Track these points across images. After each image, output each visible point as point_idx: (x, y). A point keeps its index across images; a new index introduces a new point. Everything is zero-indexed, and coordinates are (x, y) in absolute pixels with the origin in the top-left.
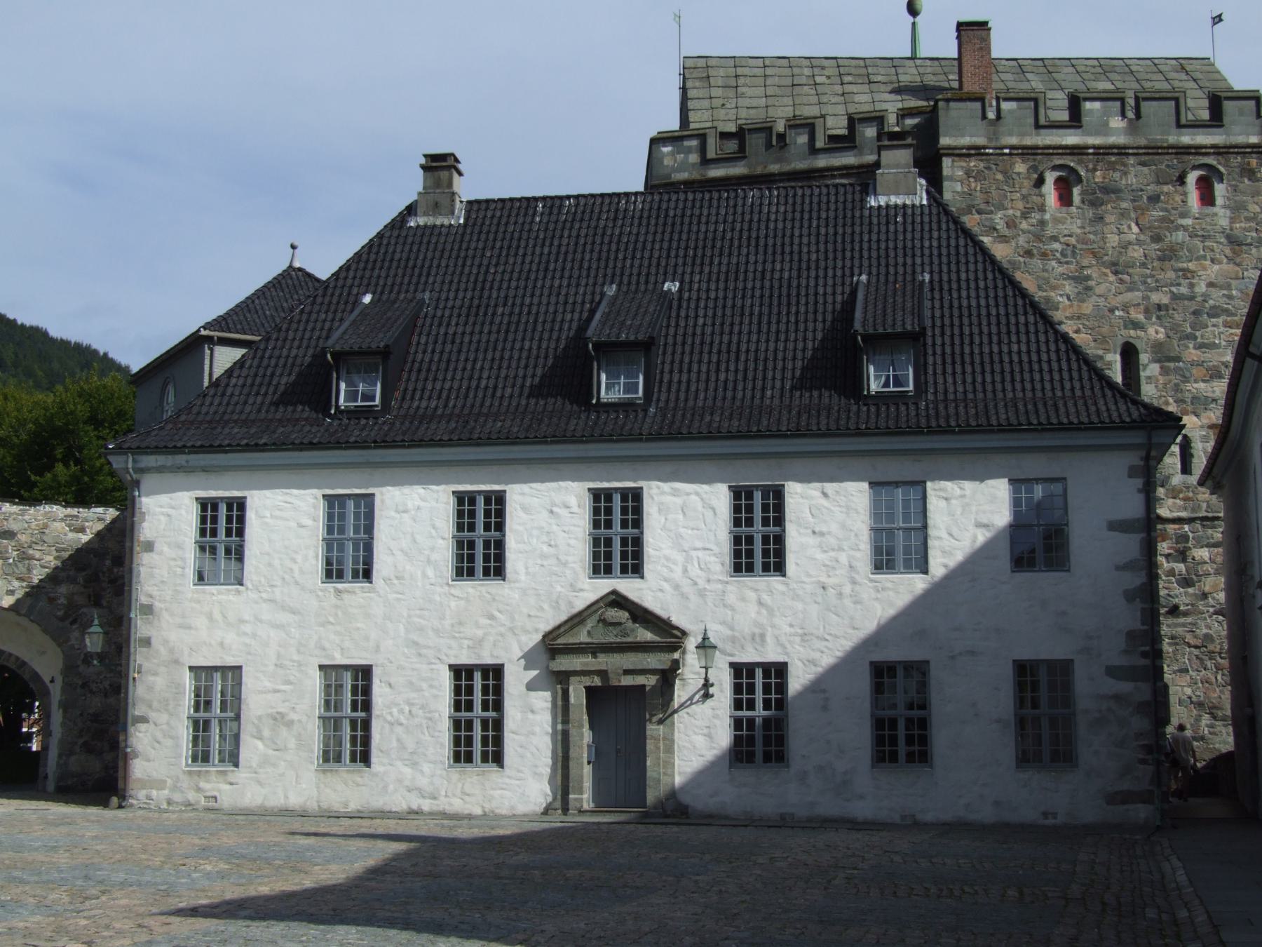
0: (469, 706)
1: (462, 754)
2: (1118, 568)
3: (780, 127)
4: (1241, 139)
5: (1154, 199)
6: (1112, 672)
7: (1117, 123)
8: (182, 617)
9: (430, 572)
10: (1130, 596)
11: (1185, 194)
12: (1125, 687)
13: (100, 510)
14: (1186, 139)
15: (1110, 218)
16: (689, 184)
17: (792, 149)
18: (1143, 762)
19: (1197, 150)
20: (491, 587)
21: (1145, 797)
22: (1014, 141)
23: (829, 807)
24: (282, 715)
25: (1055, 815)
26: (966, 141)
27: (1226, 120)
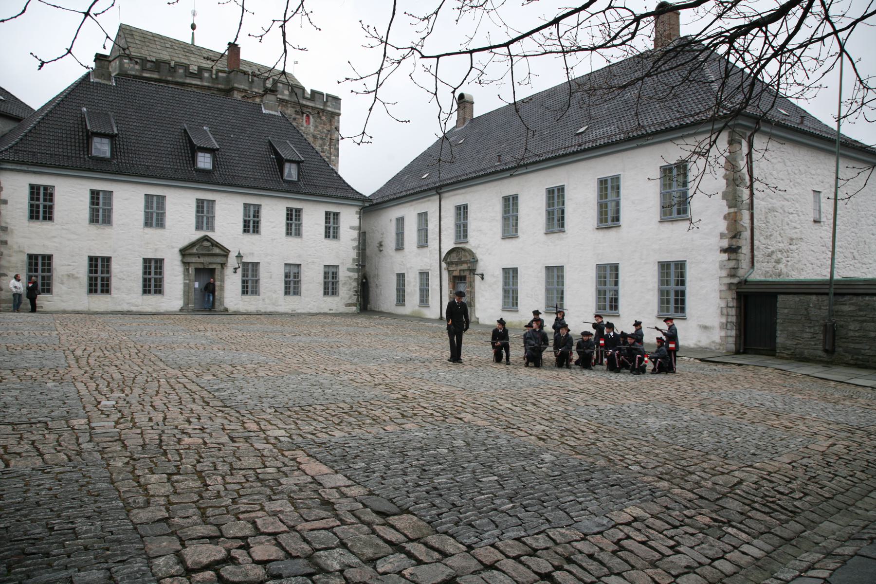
0: (150, 273)
1: (146, 291)
3: (172, 64)
6: (349, 270)
12: (351, 274)
16: (135, 77)
20: (255, 237)
21: (354, 305)
22: (256, 90)
23: (270, 309)
24: (73, 275)
26: (242, 87)
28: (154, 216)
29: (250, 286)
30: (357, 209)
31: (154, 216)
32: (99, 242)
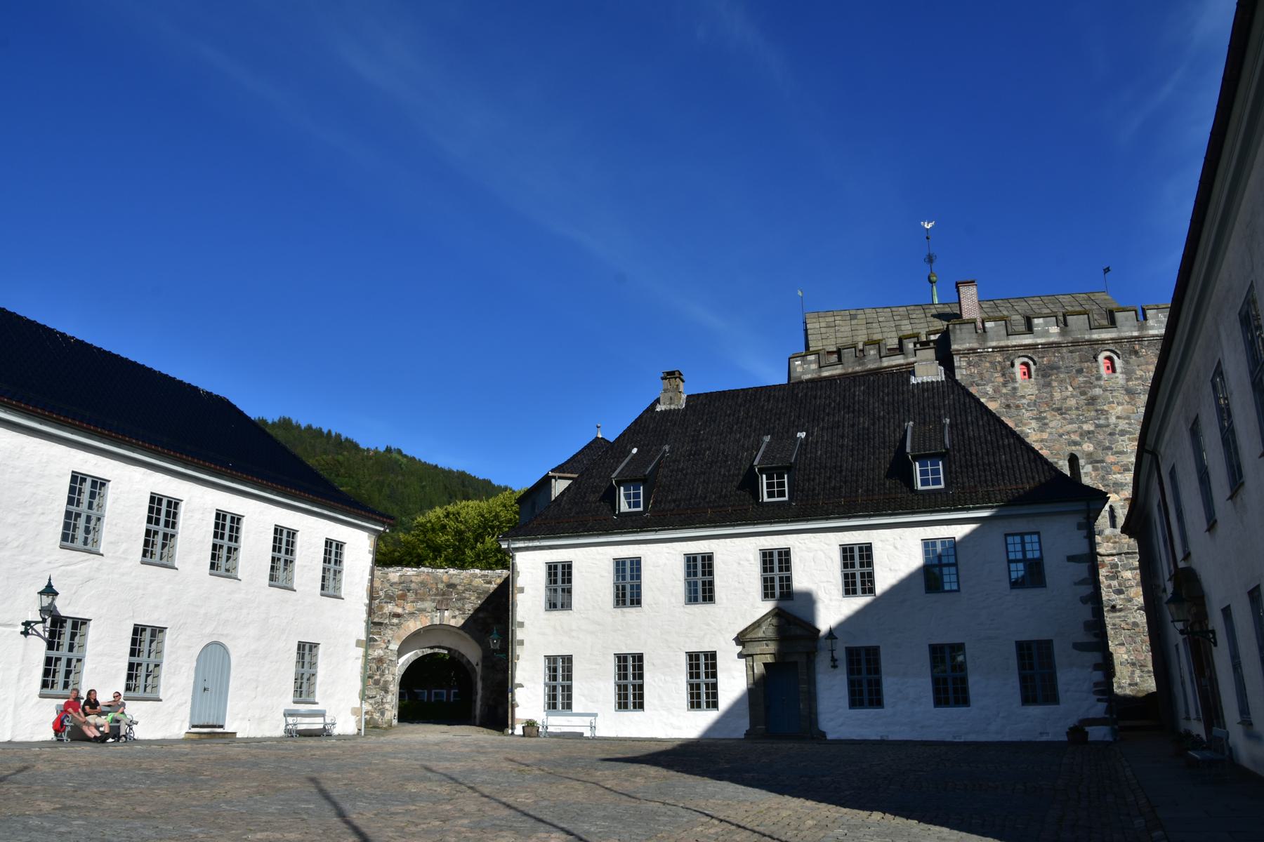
0: (698, 676)
2: (1075, 584)
4: (1128, 334)
5: (1080, 371)
7: (1054, 330)
11: (1098, 367)
14: (1095, 336)
15: (1055, 384)
17: (868, 358)
18: (1099, 700)
19: (1103, 342)
22: (994, 344)
25: (1047, 734)
26: (967, 346)
27: (1118, 324)
28: (700, 582)
29: (866, 691)
31: (700, 582)
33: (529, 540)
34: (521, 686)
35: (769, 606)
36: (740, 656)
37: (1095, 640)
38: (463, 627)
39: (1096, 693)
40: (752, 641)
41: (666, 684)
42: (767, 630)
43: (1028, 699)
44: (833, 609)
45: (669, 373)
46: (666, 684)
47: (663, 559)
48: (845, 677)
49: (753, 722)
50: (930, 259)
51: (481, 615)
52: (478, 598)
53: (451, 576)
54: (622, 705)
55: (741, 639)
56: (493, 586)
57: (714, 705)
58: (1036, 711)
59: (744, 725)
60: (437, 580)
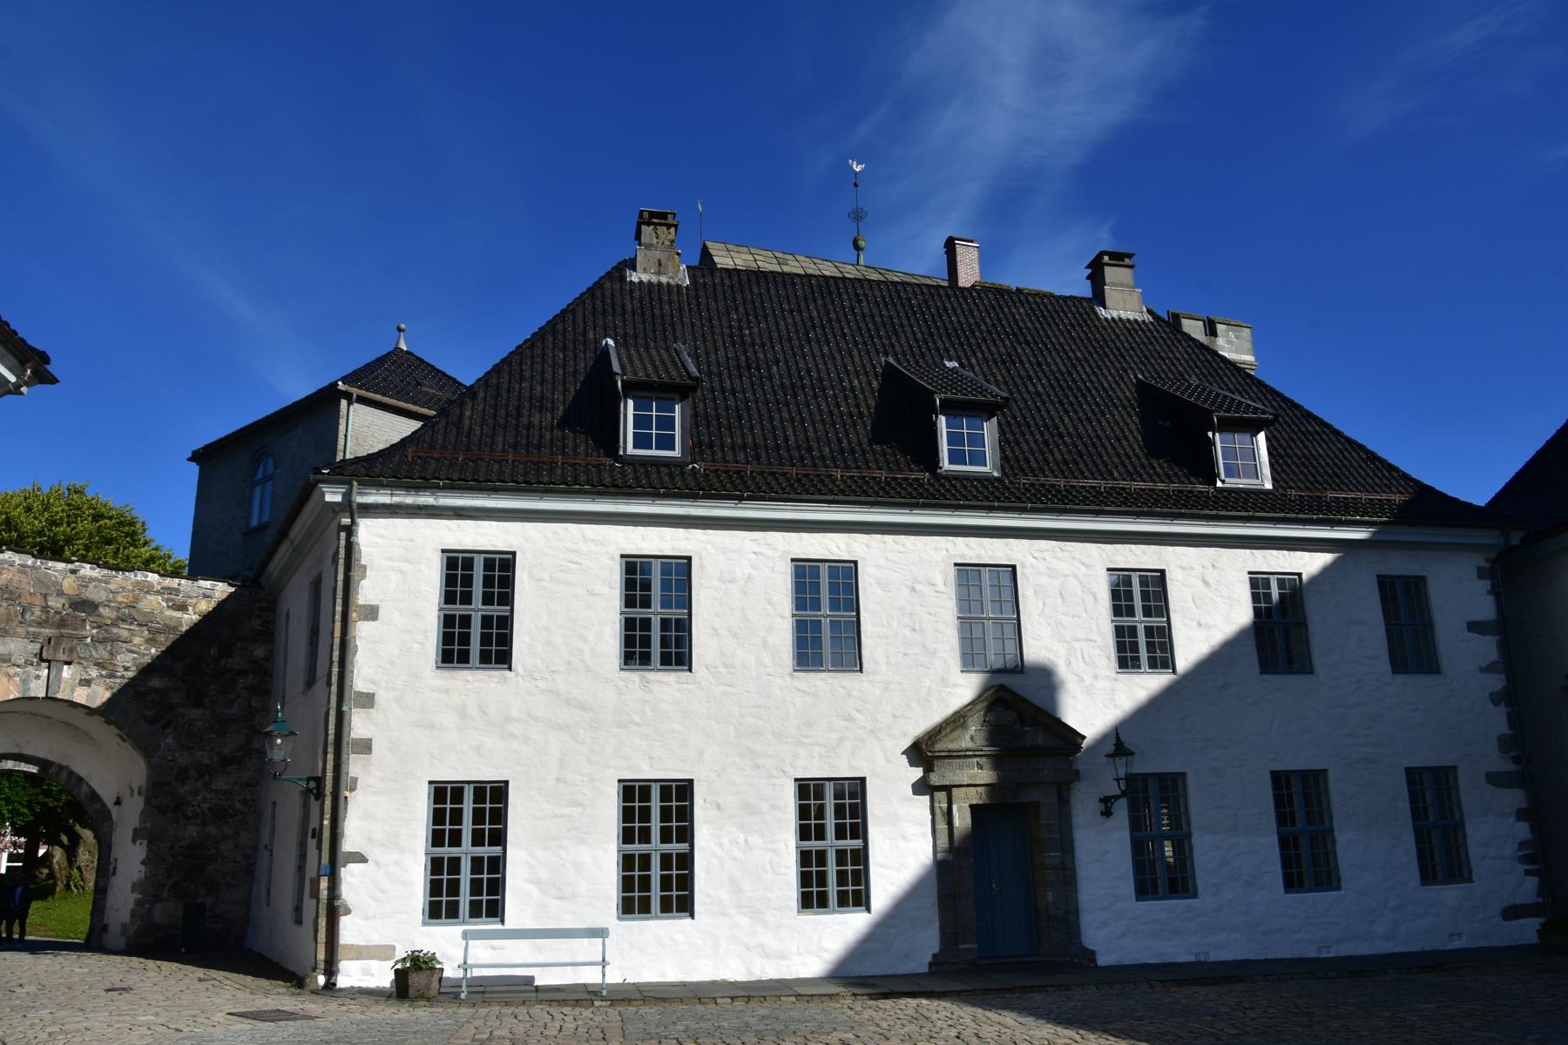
2: (1482, 670)
8: (407, 717)
9: (767, 660)
10: (1495, 699)
13: (207, 584)
18: (1528, 873)
30: (1479, 560)
32: (660, 727)
33: (409, 488)
34: (362, 859)
35: (965, 688)
36: (921, 787)
37: (1513, 767)
38: (108, 711)
39: (1522, 859)
40: (952, 755)
41: (745, 851)
42: (972, 736)
43: (1428, 875)
44: (1097, 698)
45: (653, 214)
46: (745, 851)
47: (742, 569)
48: (1125, 835)
49: (949, 936)
50: (857, 216)
51: (155, 683)
52: (151, 641)
53: (86, 582)
54: (634, 902)
55: (921, 752)
56: (190, 618)
57: (860, 900)
58: (1450, 893)
59: (926, 942)
60: (48, 587)
